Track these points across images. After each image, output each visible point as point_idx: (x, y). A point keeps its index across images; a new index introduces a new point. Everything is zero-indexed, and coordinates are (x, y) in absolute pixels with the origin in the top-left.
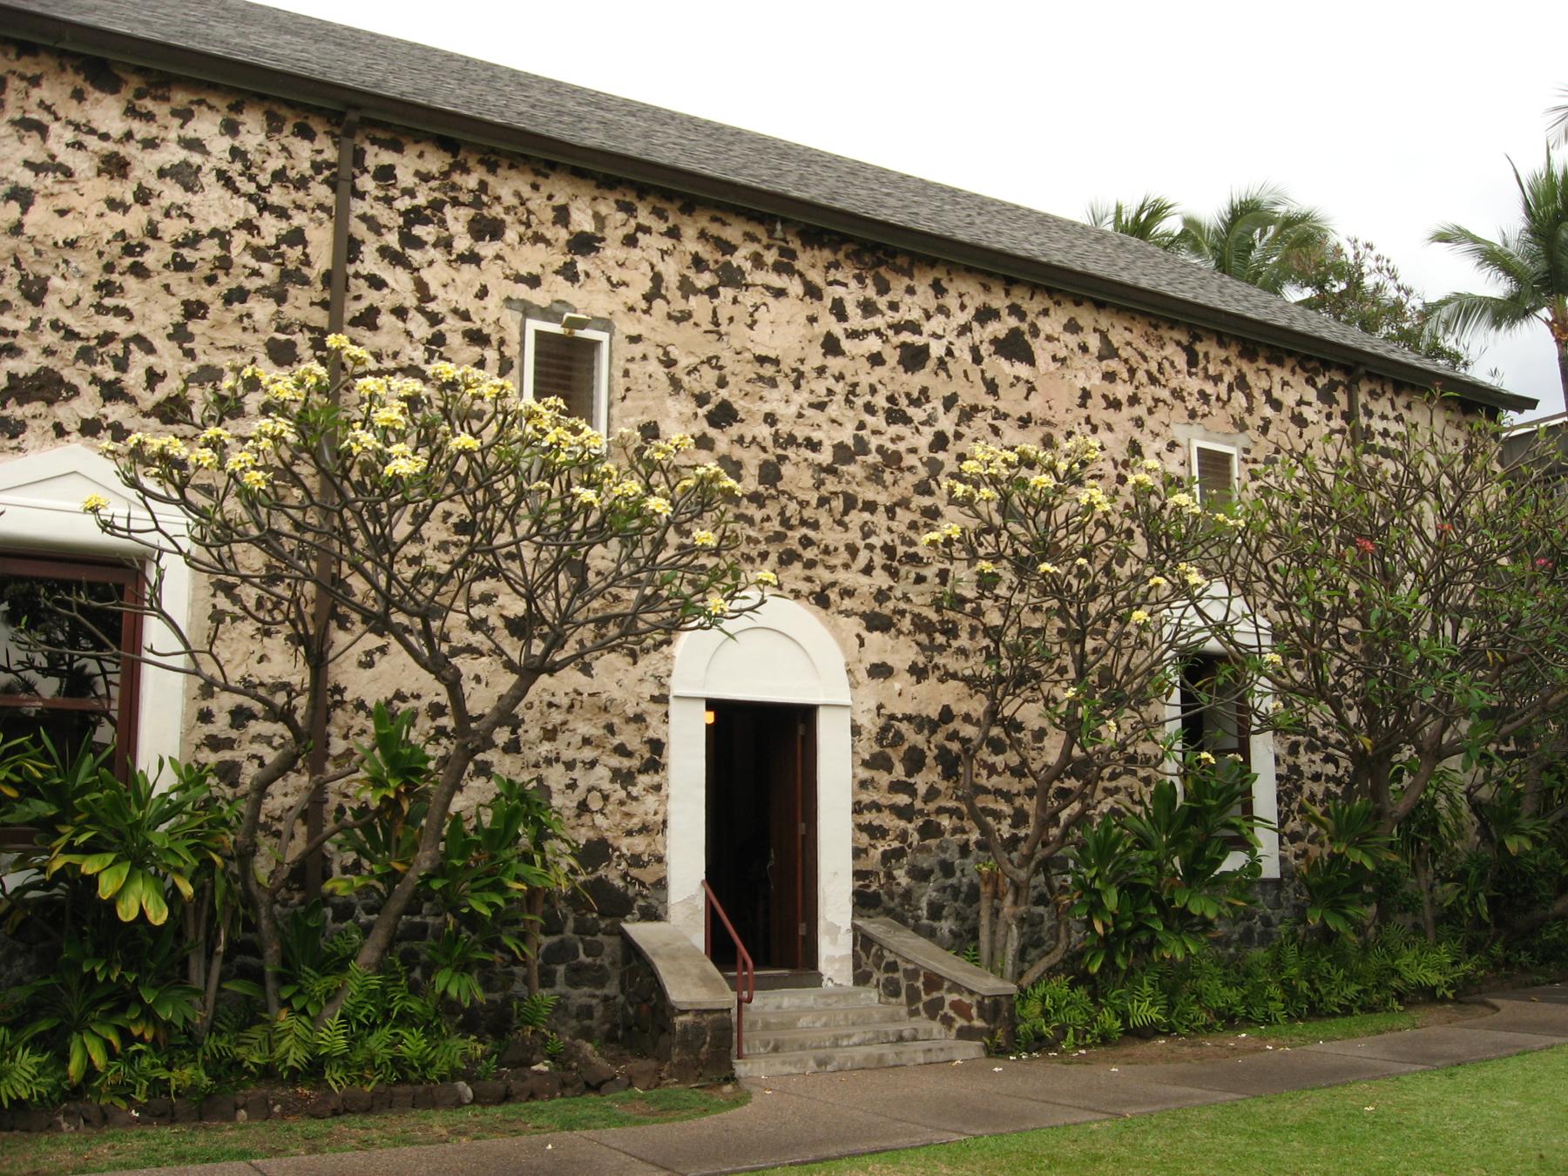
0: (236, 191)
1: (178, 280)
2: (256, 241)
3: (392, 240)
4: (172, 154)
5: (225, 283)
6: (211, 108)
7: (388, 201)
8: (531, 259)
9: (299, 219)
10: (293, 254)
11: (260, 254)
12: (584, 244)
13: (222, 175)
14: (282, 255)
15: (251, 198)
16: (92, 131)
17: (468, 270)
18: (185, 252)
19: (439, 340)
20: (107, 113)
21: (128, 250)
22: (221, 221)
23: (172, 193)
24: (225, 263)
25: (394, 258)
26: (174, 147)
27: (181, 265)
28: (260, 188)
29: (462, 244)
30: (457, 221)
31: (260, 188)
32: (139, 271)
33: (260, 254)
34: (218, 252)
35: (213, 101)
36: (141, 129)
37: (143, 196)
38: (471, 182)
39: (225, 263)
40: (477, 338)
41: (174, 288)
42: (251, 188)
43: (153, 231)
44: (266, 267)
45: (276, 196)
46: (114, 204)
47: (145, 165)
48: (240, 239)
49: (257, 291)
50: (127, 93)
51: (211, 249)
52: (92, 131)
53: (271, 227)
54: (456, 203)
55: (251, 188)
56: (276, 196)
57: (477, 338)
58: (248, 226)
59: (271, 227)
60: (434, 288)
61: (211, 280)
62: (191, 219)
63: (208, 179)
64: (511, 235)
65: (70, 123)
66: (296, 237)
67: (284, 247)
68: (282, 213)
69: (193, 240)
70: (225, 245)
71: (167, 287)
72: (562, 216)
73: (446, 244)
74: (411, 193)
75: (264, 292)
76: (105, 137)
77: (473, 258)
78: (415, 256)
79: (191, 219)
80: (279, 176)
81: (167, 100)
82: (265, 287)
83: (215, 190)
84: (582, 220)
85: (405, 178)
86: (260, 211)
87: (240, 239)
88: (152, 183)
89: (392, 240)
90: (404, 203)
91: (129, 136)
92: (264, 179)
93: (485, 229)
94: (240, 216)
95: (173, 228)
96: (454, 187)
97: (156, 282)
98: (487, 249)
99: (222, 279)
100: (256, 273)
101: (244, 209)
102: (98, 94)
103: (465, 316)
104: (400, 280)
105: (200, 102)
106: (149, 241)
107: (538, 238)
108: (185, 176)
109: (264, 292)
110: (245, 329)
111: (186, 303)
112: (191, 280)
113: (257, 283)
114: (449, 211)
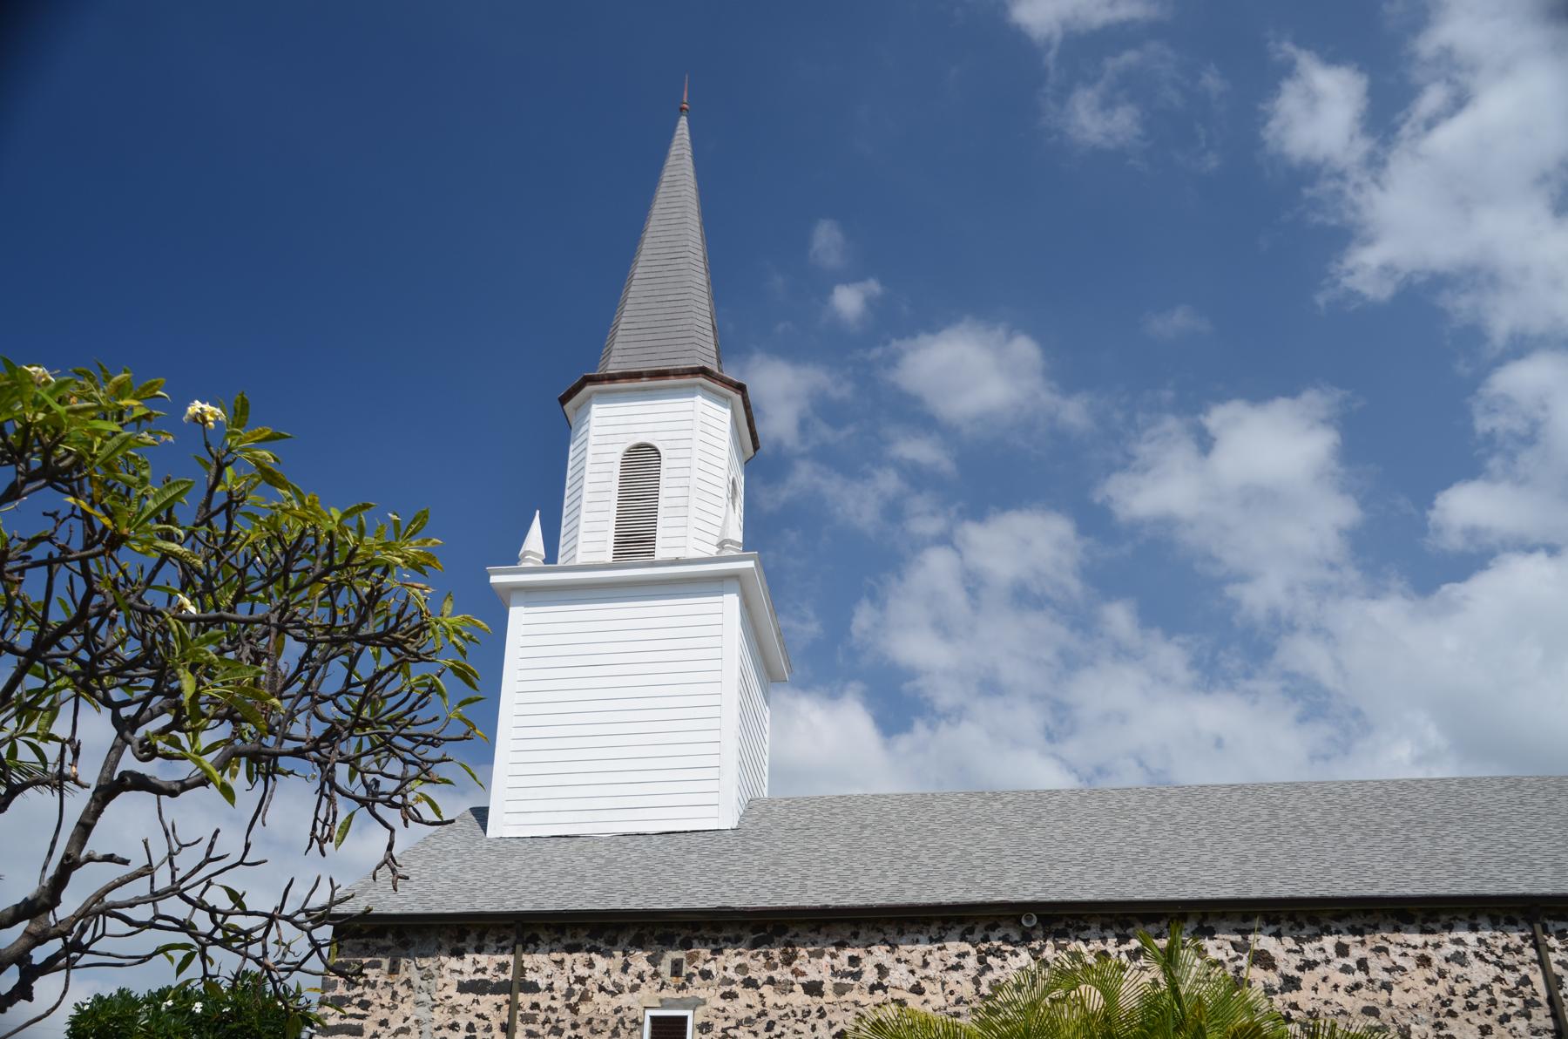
0: (1487, 961)
1: (1472, 1015)
2: (1505, 987)
4: (1449, 949)
5: (1498, 1012)
6: (1460, 920)
9: (1524, 970)
10: (1527, 990)
11: (1509, 993)
13: (1476, 954)
14: (1521, 992)
15: (1496, 964)
16: (1409, 946)
18: (1471, 999)
21: (1444, 1004)
22: (1486, 980)
23: (1456, 969)
24: (1493, 1002)
26: (1449, 945)
27: (1472, 1007)
28: (1498, 957)
31: (1498, 957)
32: (1452, 1014)
33: (1509, 993)
34: (1488, 997)
35: (1460, 916)
36: (1432, 939)
37: (1442, 974)
41: (1472, 1020)
42: (1494, 958)
44: (1515, 1000)
45: (1508, 960)
46: (1430, 981)
47: (1437, 958)
48: (1496, 987)
49: (1515, 1014)
51: (1483, 996)
52: (1409, 946)
53: (1511, 978)
55: (1494, 958)
56: (1508, 960)
58: (1498, 979)
59: (1511, 978)
61: (1489, 1012)
62: (1469, 981)
63: (1471, 957)
65: (1397, 944)
66: (1526, 981)
67: (1521, 988)
68: (1513, 969)
69: (1473, 993)
70: (1490, 992)
71: (1468, 1020)
75: (1517, 1014)
76: (1415, 947)
79: (1469, 981)
80: (1506, 949)
81: (1438, 921)
82: (1518, 1011)
83: (1477, 963)
86: (1502, 970)
87: (1496, 987)
88: (1445, 966)
91: (1426, 944)
92: (1499, 952)
94: (1493, 975)
95: (1461, 988)
97: (1461, 1018)
99: (1494, 1010)
100: (1511, 1004)
101: (1495, 971)
102: (1405, 926)
105: (1454, 919)
106: (1452, 997)
108: (1459, 959)
109: (1519, 1014)
110: (1515, 1037)
111: (1480, 1027)
112: (1479, 1014)
113: (1511, 1010)
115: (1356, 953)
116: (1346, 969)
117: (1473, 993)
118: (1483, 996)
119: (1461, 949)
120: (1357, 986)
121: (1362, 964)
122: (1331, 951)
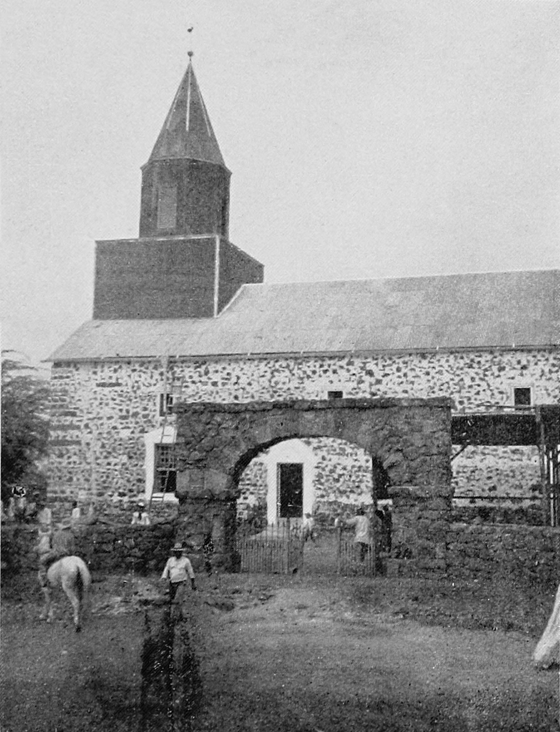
3: (482, 376)
4: (438, 369)
7: (480, 368)
8: (512, 373)
10: (461, 383)
12: (524, 368)
17: (498, 379)
19: (493, 394)
20: (425, 363)
23: (437, 376)
24: (449, 388)
25: (482, 379)
29: (496, 374)
30: (495, 369)
33: (455, 384)
36: (432, 365)
38: (496, 360)
39: (449, 388)
40: (501, 393)
43: (435, 384)
48: (451, 383)
50: (428, 359)
53: (457, 379)
54: (495, 365)
57: (501, 393)
60: (491, 385)
63: (444, 372)
64: (507, 369)
72: (519, 362)
73: (493, 374)
74: (484, 365)
75: (456, 392)
76: (425, 368)
77: (499, 376)
78: (486, 378)
80: (458, 368)
83: (445, 374)
84: (524, 362)
85: (483, 362)
87: (451, 383)
89: (482, 376)
90: (483, 368)
93: (501, 369)
95: (439, 383)
96: (494, 362)
98: (502, 373)
103: (497, 388)
104: (484, 385)
107: (514, 368)
108: (440, 372)
109: (456, 392)
114: (493, 367)
115: (404, 370)
116: (399, 377)
117: (442, 385)
118: (446, 385)
119: (441, 368)
120: (402, 383)
121: (405, 375)
122: (395, 370)
